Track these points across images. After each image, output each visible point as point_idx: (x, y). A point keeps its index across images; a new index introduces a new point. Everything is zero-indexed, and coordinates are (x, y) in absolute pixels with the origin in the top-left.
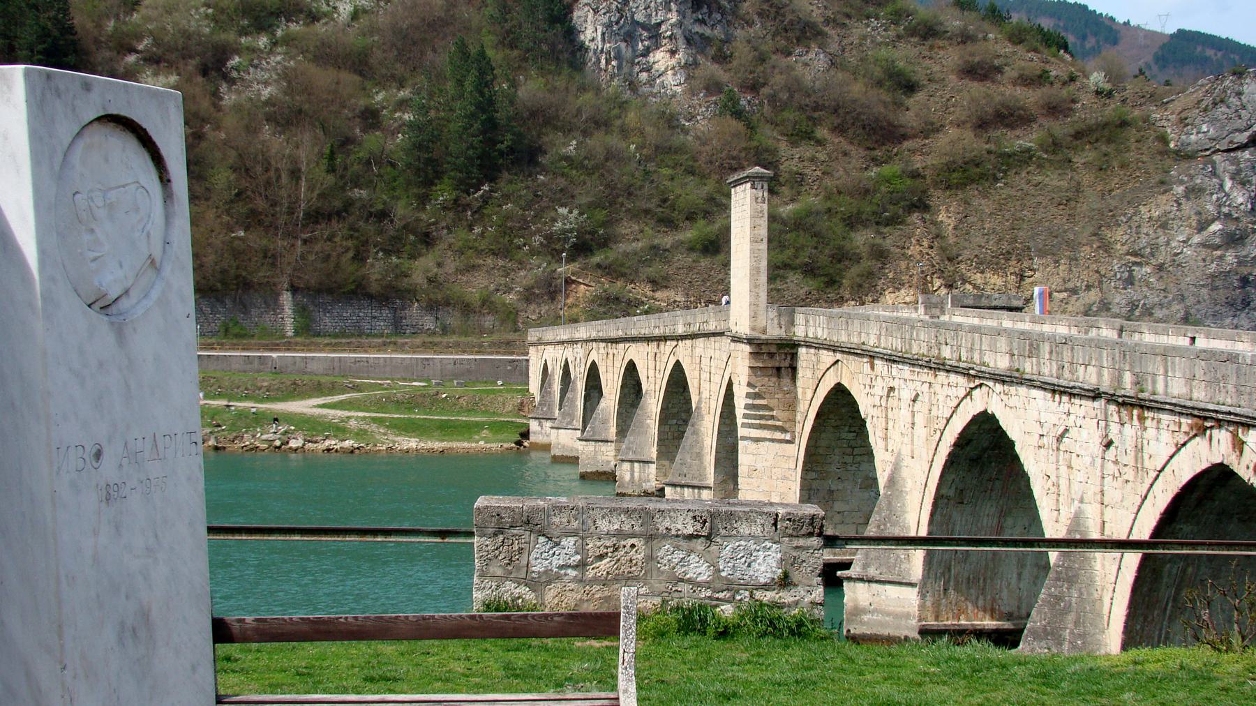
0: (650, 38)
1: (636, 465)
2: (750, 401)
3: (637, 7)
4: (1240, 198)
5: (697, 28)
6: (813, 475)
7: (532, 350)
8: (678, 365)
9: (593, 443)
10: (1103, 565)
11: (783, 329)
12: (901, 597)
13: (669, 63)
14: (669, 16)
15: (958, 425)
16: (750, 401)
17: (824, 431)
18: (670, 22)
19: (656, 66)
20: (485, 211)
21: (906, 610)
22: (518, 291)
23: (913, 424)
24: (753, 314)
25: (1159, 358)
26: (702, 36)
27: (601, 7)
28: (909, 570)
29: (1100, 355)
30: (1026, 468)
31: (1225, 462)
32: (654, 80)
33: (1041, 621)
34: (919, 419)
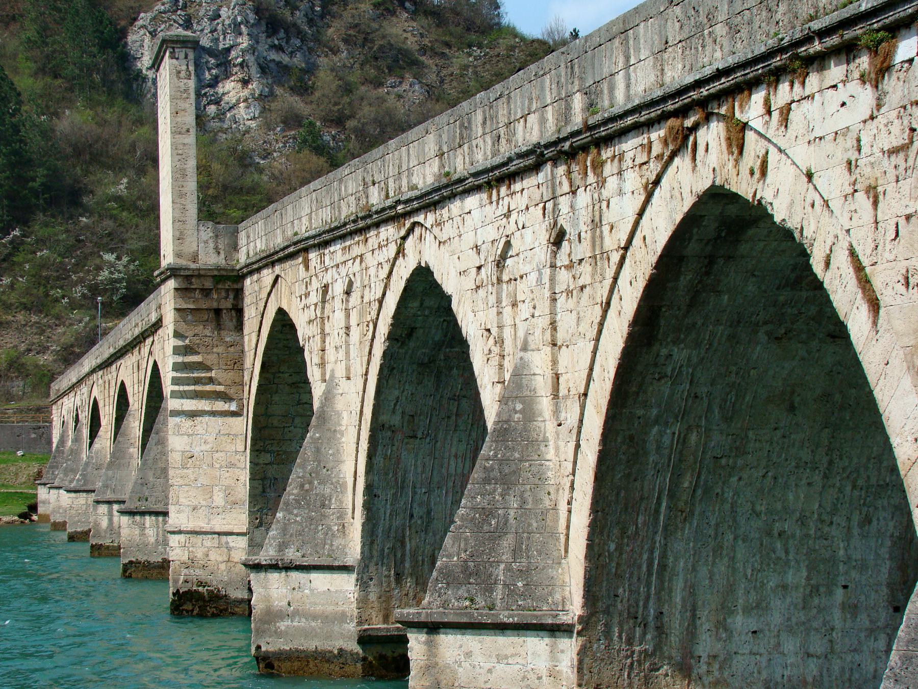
0: (218, 66)
2: (180, 359)
3: (202, 30)
5: (274, 56)
6: (267, 458)
9: (84, 494)
10: (557, 449)
11: (222, 256)
12: (332, 589)
13: (242, 94)
14: (240, 40)
16: (180, 359)
17: (276, 392)
18: (241, 47)
19: (226, 98)
20: (15, 259)
21: (340, 608)
22: (54, 350)
24: (178, 234)
26: (279, 64)
27: (159, 29)
28: (345, 546)
32: (224, 114)
33: (458, 555)
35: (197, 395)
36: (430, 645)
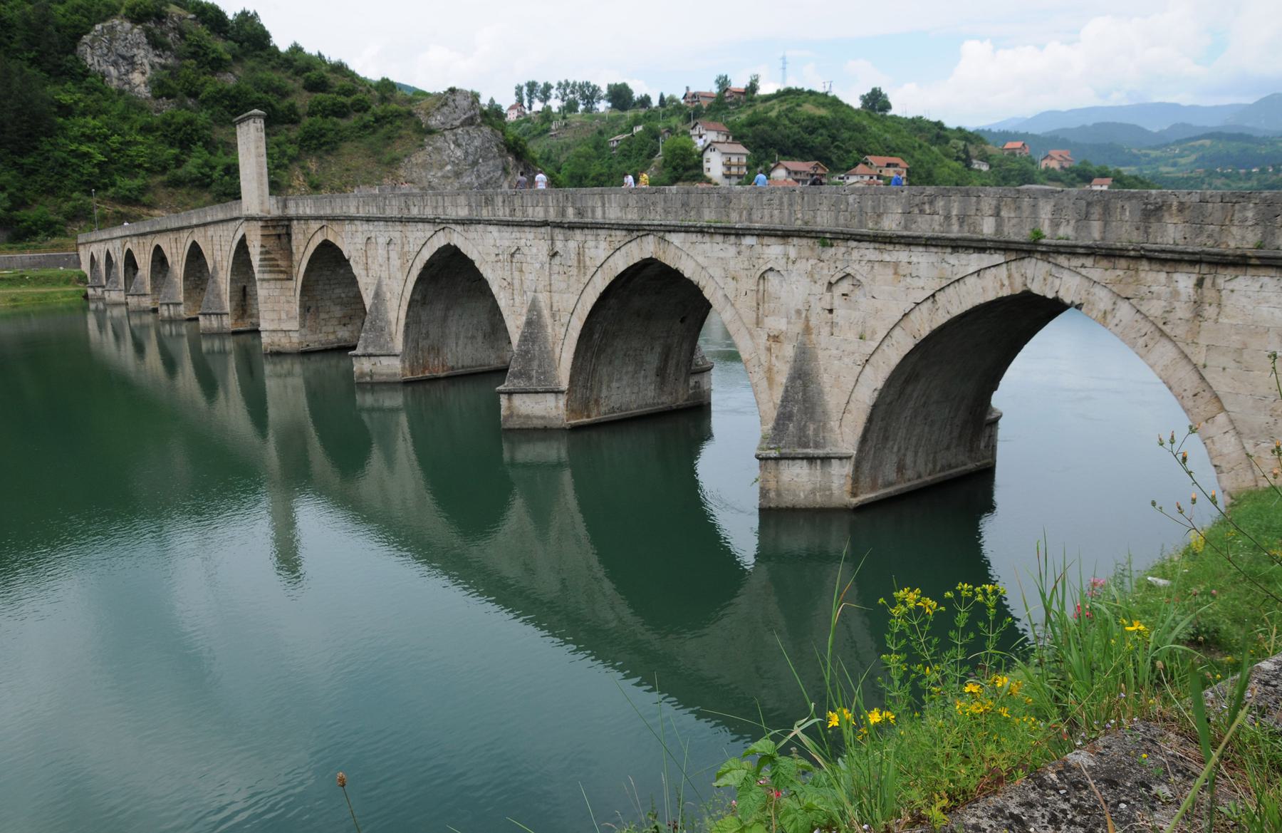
0: (128, 64)
1: (171, 307)
2: (263, 257)
4: (459, 153)
6: (307, 298)
7: (81, 248)
8: (195, 246)
11: (280, 210)
14: (140, 51)
15: (426, 255)
23: (389, 258)
25: (597, 196)
26: (160, 64)
28: (393, 347)
29: (547, 200)
30: (485, 276)
31: (654, 257)
34: (394, 255)
35: (270, 272)
36: (509, 399)
